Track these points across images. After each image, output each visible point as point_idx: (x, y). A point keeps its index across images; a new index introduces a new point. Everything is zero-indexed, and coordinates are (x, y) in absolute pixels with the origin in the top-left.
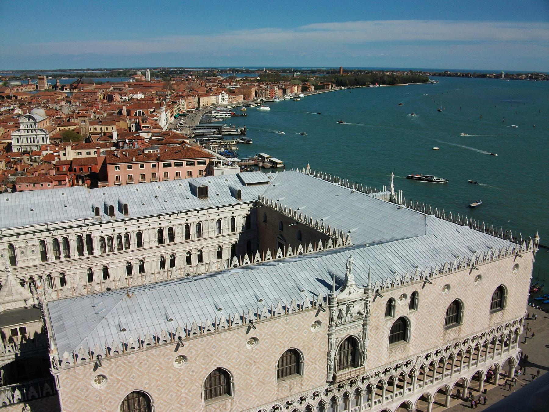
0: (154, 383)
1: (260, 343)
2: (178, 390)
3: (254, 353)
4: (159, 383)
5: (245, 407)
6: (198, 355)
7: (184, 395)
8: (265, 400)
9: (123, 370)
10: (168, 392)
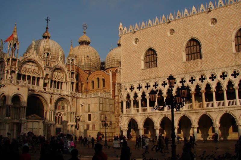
0: (158, 44)
1: (218, 22)
2: (170, 49)
3: (214, 28)
4: (160, 44)
5: (211, 66)
6: (180, 29)
7: (172, 53)
8: (225, 64)
9: (145, 36)
10: (164, 50)
